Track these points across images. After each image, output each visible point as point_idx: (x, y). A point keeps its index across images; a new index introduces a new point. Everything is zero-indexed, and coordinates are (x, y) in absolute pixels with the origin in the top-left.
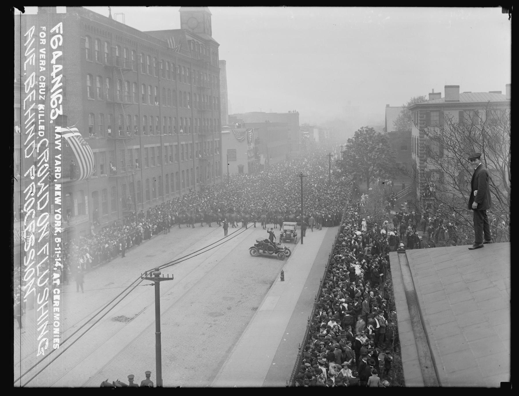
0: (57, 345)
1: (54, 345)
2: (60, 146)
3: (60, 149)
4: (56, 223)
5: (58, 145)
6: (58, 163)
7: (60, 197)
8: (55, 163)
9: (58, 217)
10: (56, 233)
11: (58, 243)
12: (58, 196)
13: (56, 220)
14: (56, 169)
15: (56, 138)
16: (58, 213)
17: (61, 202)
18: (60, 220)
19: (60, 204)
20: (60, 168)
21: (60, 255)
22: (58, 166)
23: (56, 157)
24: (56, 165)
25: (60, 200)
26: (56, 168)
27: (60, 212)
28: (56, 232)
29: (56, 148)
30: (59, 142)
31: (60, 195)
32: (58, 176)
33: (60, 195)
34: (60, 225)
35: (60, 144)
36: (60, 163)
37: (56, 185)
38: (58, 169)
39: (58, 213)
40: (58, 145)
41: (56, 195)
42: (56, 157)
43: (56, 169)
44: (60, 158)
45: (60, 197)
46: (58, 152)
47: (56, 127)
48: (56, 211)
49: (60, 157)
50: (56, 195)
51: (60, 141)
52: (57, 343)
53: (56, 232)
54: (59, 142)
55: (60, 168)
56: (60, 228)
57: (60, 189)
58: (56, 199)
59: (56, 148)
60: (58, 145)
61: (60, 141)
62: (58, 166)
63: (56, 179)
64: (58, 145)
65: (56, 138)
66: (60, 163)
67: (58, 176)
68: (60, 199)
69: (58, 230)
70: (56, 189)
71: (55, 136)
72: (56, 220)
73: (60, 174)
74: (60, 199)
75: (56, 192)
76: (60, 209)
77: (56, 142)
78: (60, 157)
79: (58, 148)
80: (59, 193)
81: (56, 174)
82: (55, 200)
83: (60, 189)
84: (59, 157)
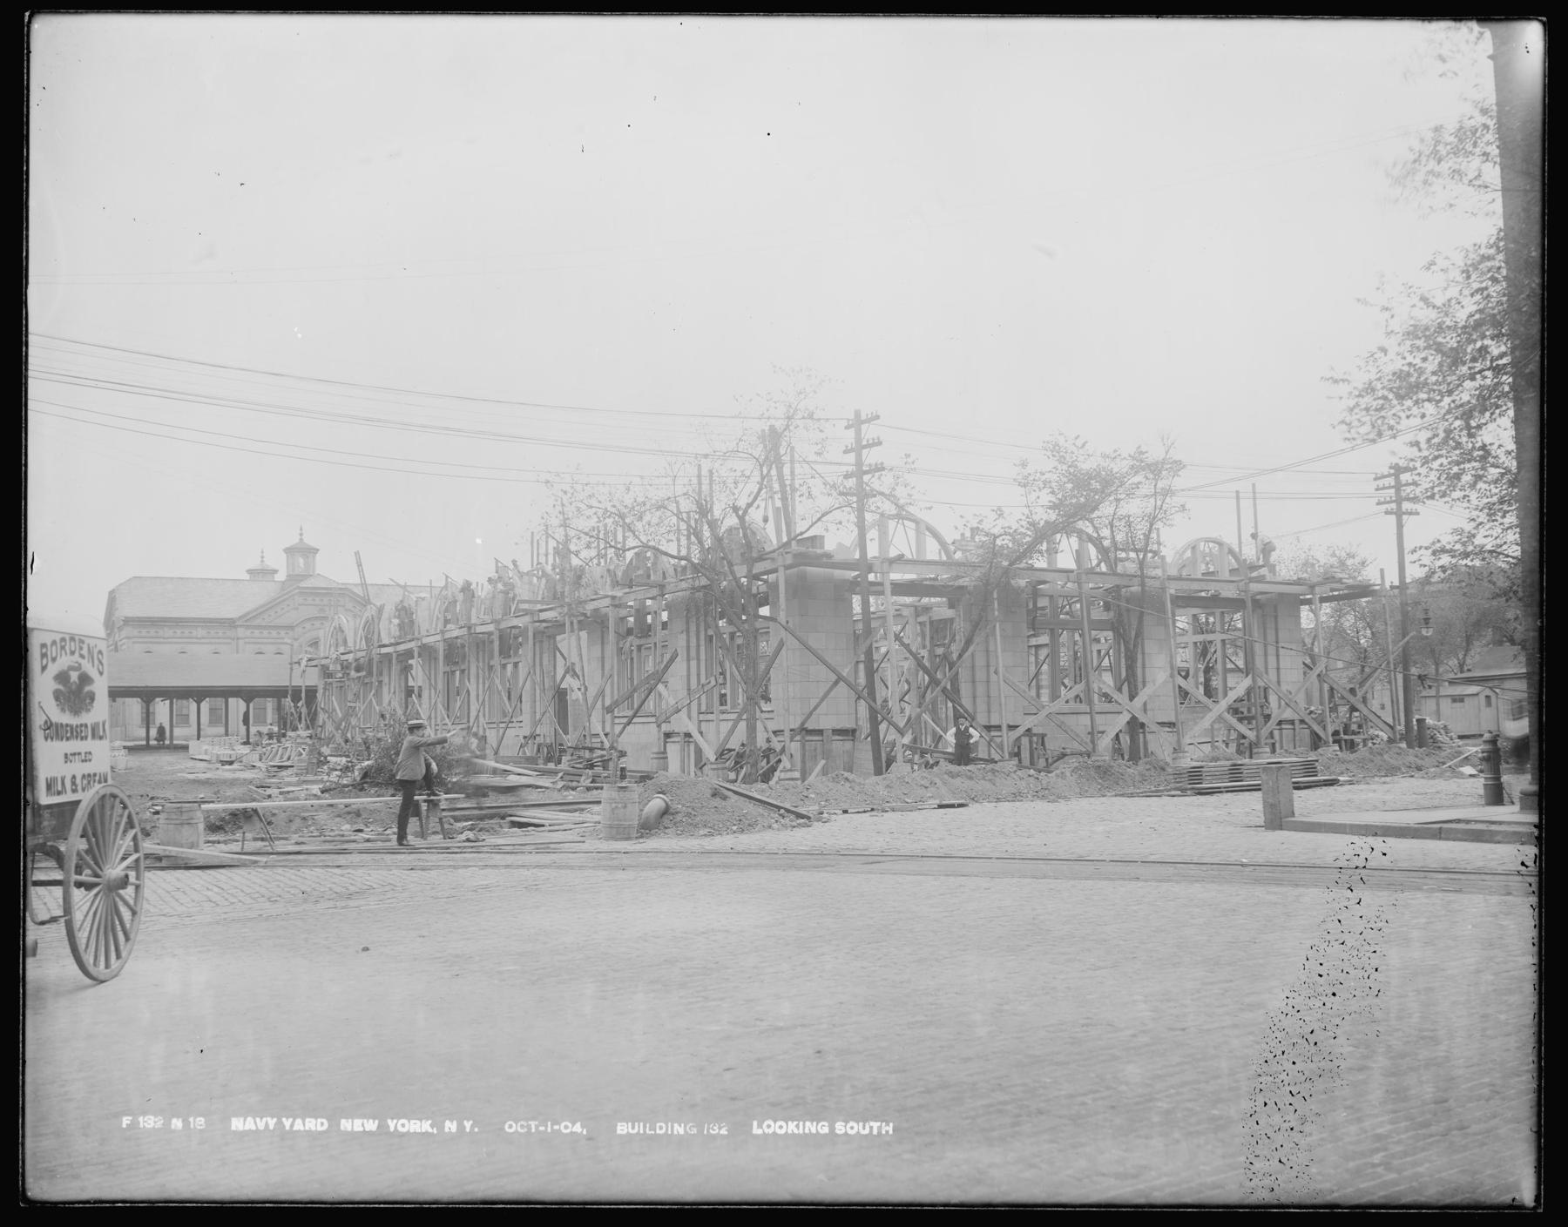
2: (269, 1119)
3: (275, 1120)
6: (298, 1125)
12: (363, 1125)
23: (287, 1128)
25: (371, 1121)
27: (395, 1121)
28: (430, 1130)
34: (418, 1122)
35: (264, 1119)
36: (299, 1121)
41: (361, 1129)
42: (287, 1128)
51: (258, 1120)
55: (307, 1120)
66: (299, 1121)
67: (322, 1124)
70: (349, 1129)
73: (319, 1120)
75: (356, 1129)
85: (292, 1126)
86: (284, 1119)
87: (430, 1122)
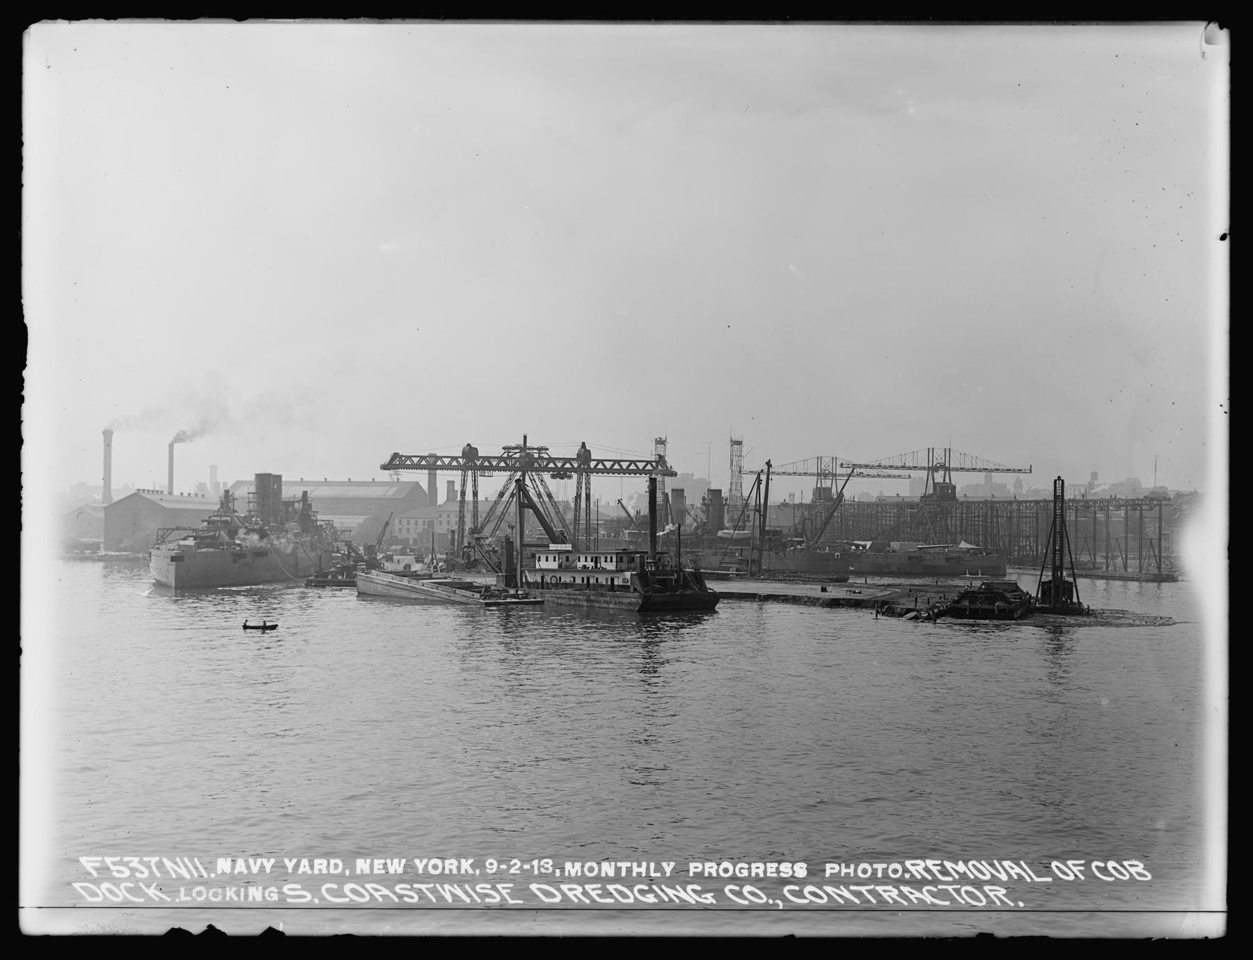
0: (781, 869)
1: (782, 875)
2: (265, 861)
3: (273, 861)
4: (451, 870)
5: (262, 867)
7: (389, 861)
8: (304, 873)
9: (435, 867)
10: (474, 871)
11: (498, 868)
13: (444, 868)
14: (320, 870)
15: (245, 872)
16: (426, 866)
17: (400, 862)
18: (443, 863)
19: (404, 861)
20: (317, 862)
21: (523, 862)
22: (312, 867)
24: (309, 872)
25: (396, 861)
26: (316, 872)
27: (425, 861)
29: (268, 871)
30: (255, 863)
31: (383, 861)
32: (336, 866)
33: (383, 861)
35: (259, 861)
36: (305, 862)
37: (358, 872)
38: (320, 867)
39: (428, 862)
40: (262, 867)
42: (290, 871)
43: (320, 870)
44: (294, 861)
45: (389, 861)
46: (279, 866)
47: (219, 871)
48: (421, 871)
49: (290, 860)
50: (383, 872)
51: (251, 861)
52: (777, 868)
53: (471, 871)
54: (255, 863)
55: (317, 862)
56: (463, 861)
57: (369, 861)
58: (392, 871)
59: (268, 871)
60: (262, 863)
61: (251, 861)
62: (312, 867)
63: (344, 870)
64: (262, 863)
65: (245, 872)
66: (305, 862)
67: (336, 866)
68: (392, 864)
69: (466, 865)
70: (367, 871)
71: (241, 873)
72: (444, 868)
73: (332, 861)
74: (392, 864)
75: (376, 871)
76: (417, 861)
77: (255, 870)
78: (290, 860)
79: (269, 864)
80: (378, 863)
81: (332, 871)
82: (393, 872)
83: (369, 861)
84: (290, 865)
85: (297, 866)
86: (286, 861)
87: (471, 861)
